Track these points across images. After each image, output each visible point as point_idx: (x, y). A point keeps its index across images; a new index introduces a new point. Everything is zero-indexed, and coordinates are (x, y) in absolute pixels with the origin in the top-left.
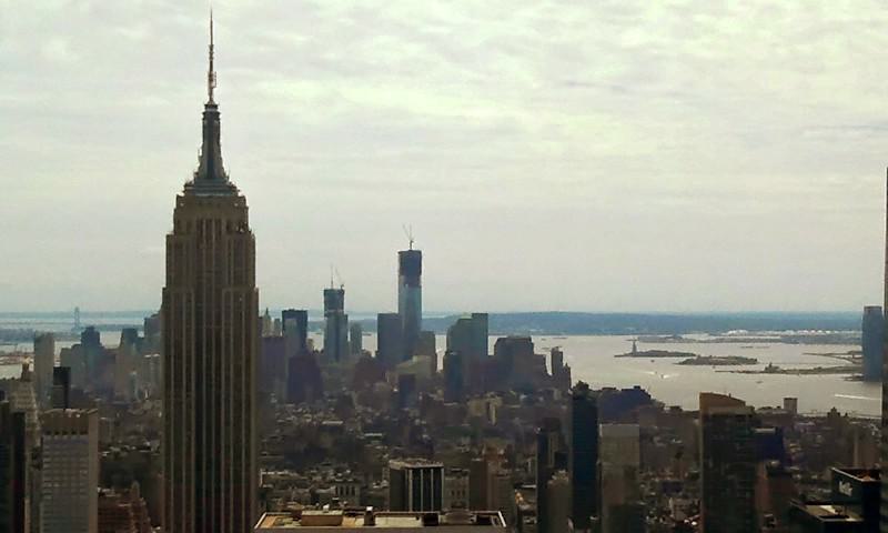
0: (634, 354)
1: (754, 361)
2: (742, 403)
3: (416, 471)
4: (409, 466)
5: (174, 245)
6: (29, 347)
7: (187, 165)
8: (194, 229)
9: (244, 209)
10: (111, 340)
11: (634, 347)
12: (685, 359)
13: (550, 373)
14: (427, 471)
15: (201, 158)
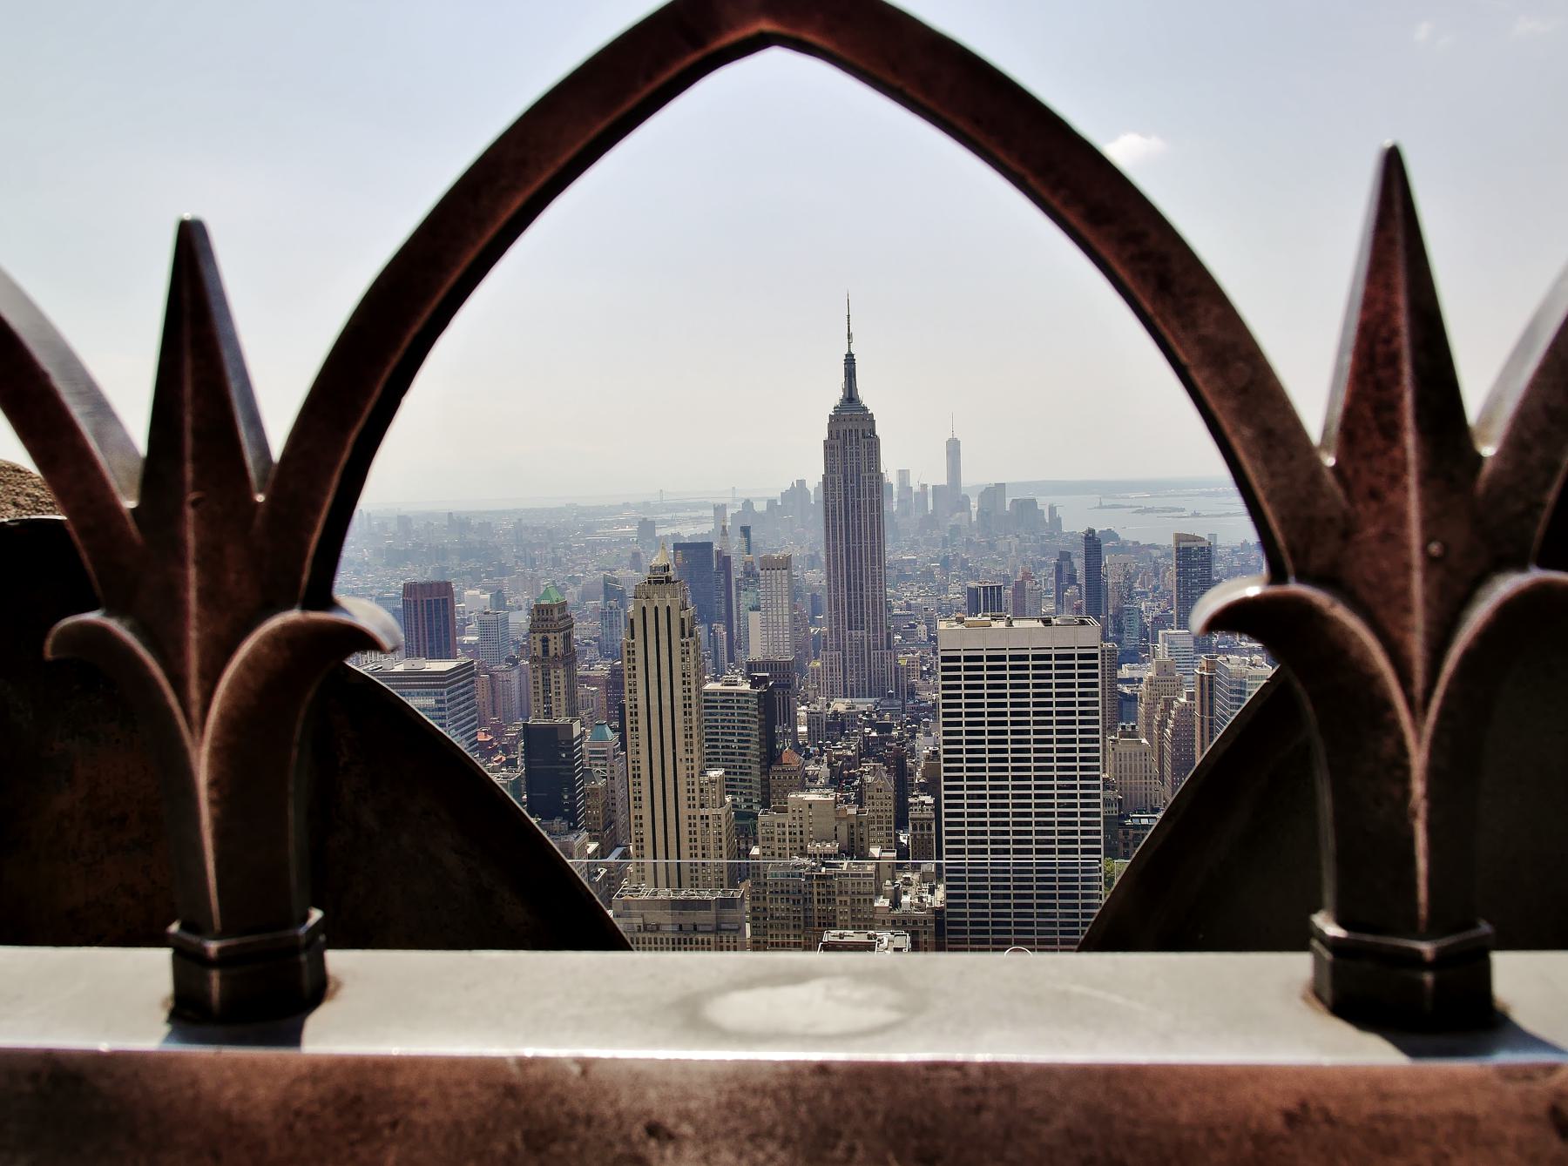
0: (1101, 507)
1: (1183, 510)
2: (1196, 539)
3: (985, 588)
4: (980, 585)
5: (828, 446)
6: (711, 513)
7: (836, 395)
8: (841, 435)
9: (873, 422)
10: (760, 507)
11: (1101, 503)
12: (1135, 509)
13: (1047, 521)
14: (992, 588)
15: (844, 390)
